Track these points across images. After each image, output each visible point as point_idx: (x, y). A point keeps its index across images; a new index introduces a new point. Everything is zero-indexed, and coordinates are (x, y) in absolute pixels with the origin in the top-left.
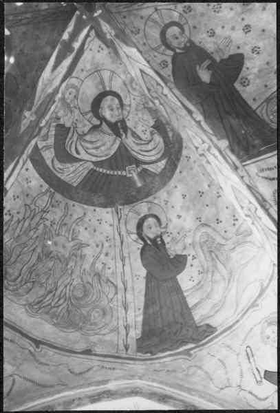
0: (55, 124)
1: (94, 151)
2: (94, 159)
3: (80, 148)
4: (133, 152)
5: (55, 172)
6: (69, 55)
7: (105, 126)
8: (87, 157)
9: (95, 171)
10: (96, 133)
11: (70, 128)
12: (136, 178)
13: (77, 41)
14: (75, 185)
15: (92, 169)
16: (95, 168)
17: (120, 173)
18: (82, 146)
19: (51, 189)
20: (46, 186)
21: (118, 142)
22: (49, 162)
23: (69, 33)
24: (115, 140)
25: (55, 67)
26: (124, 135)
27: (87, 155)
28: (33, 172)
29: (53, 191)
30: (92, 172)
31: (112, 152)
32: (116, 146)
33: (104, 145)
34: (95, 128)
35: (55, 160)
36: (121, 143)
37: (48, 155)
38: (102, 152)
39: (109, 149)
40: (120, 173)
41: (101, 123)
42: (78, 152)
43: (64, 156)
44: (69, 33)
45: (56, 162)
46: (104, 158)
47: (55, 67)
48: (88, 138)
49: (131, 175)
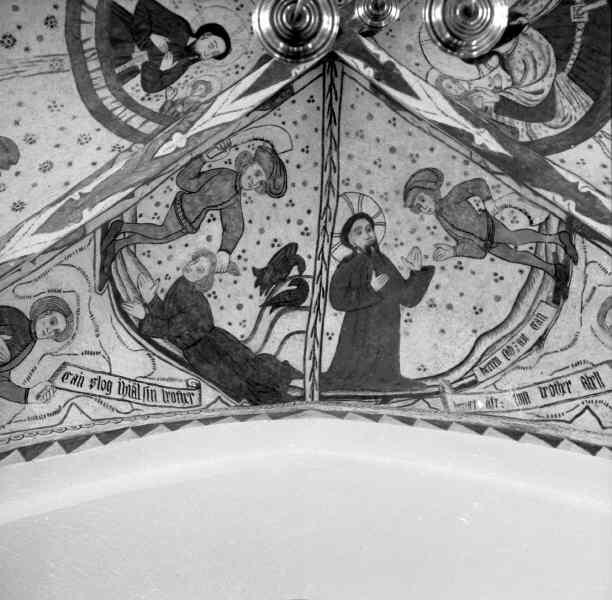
0: (494, 115)
1: (540, 69)
2: (553, 70)
3: (532, 88)
4: (550, 7)
5: (567, 127)
6: (397, 70)
7: (503, 49)
8: (548, 81)
9: (572, 71)
10: (511, 62)
11: (501, 96)
12: (591, 7)
13: (378, 56)
14: (592, 102)
15: (568, 75)
16: (567, 71)
17: (579, 33)
18: (531, 84)
19: (597, 135)
20: (591, 141)
21: (531, 31)
22: (552, 132)
23: (365, 67)
24: (525, 35)
25: (411, 93)
26: (521, 19)
27: (545, 79)
28: (571, 155)
29: (599, 133)
30: (573, 77)
31: (545, 42)
32: (536, 35)
33: (531, 53)
34: (504, 63)
35: (548, 123)
36: (532, 25)
37: (543, 131)
38: (542, 57)
39: (539, 46)
40: (579, 33)
41: (497, 53)
42: (540, 92)
43: (545, 110)
44: (365, 67)
45: (553, 122)
46: (552, 54)
47: (411, 93)
48: (518, 76)
49: (586, 15)
